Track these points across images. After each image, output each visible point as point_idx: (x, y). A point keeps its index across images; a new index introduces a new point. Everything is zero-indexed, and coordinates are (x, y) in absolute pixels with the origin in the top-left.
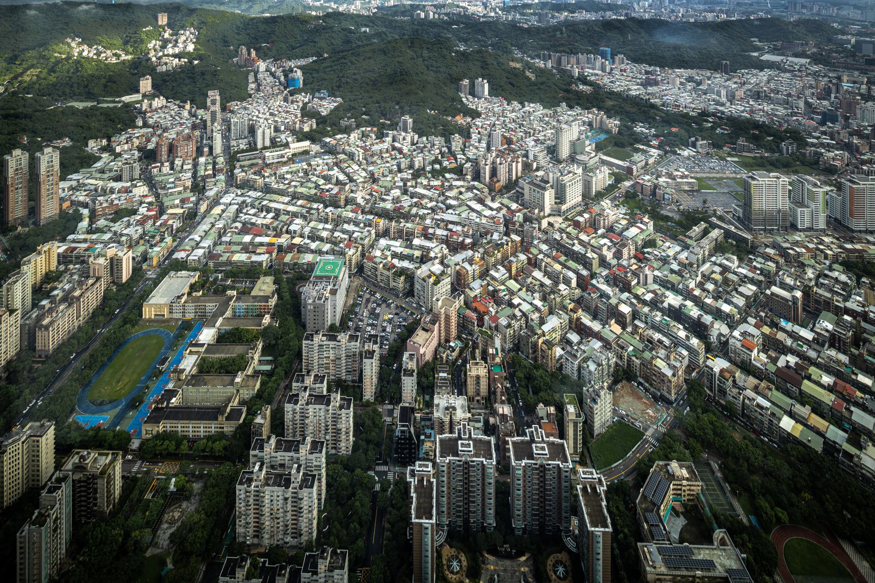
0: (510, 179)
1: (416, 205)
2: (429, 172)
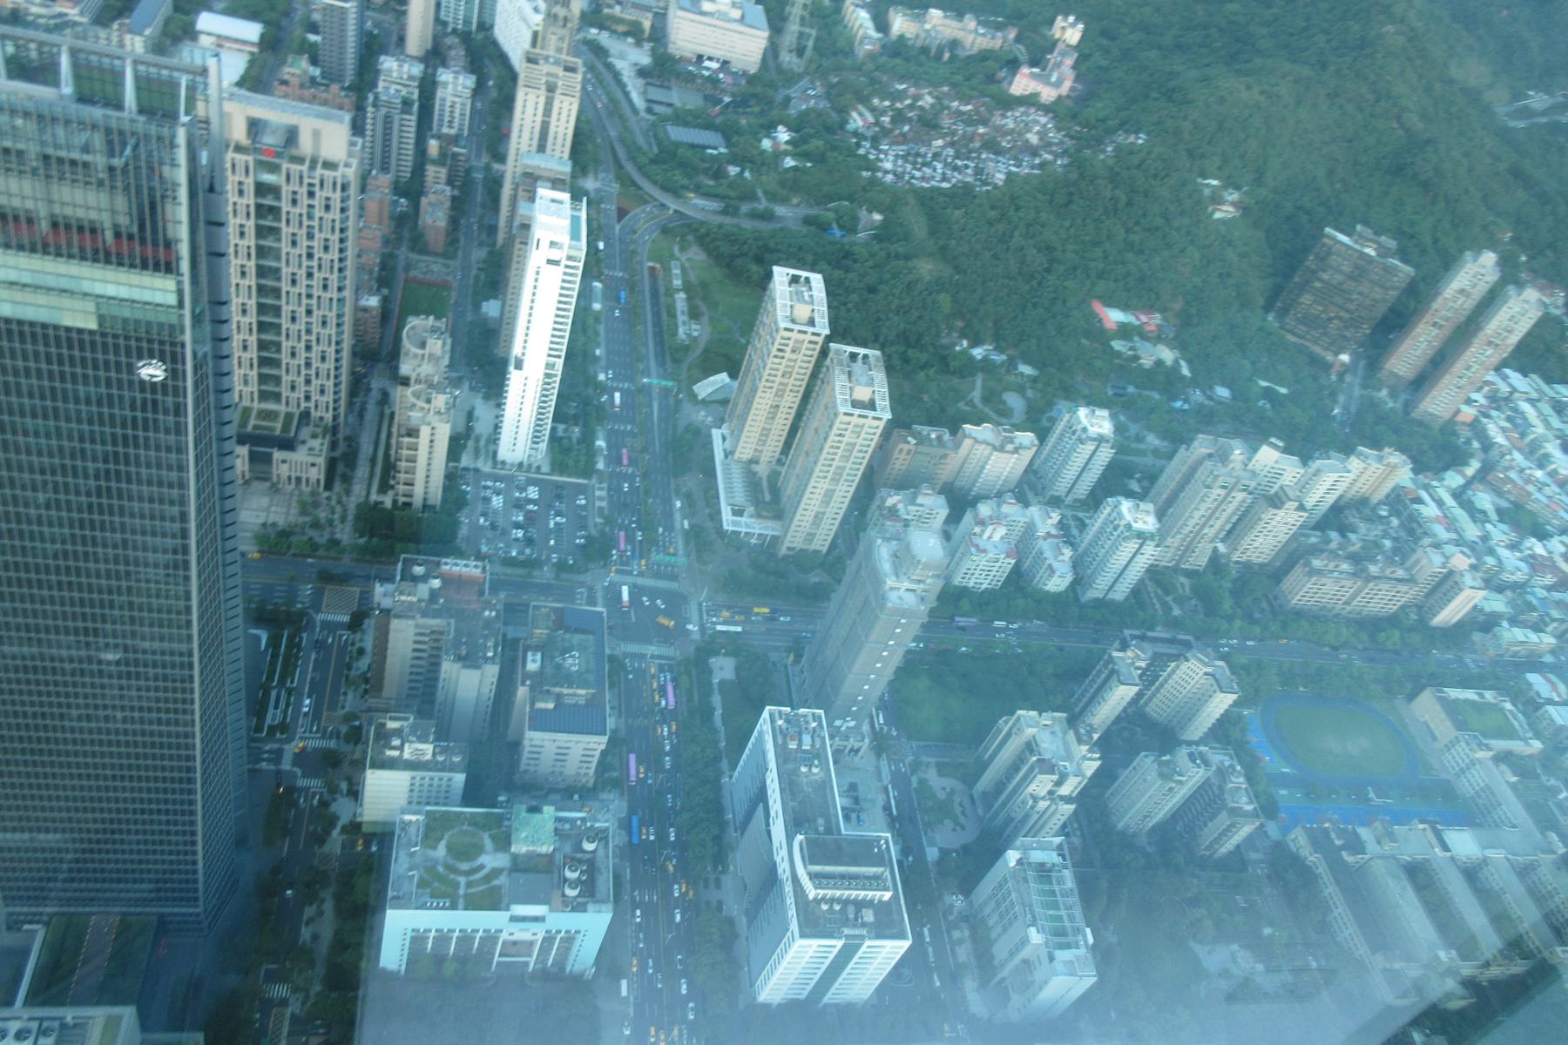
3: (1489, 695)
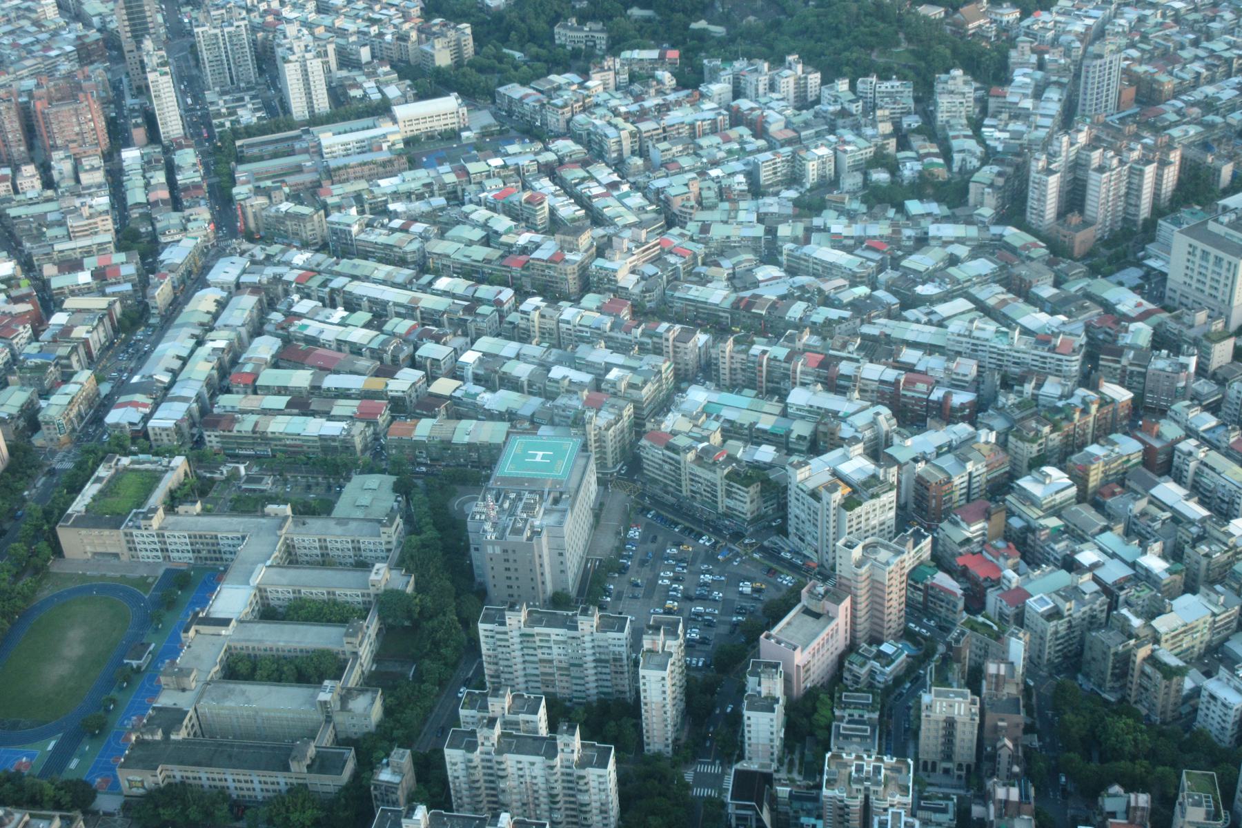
0: (1129, 220)
1: (803, 294)
2: (853, 194)
3: (103, 472)
